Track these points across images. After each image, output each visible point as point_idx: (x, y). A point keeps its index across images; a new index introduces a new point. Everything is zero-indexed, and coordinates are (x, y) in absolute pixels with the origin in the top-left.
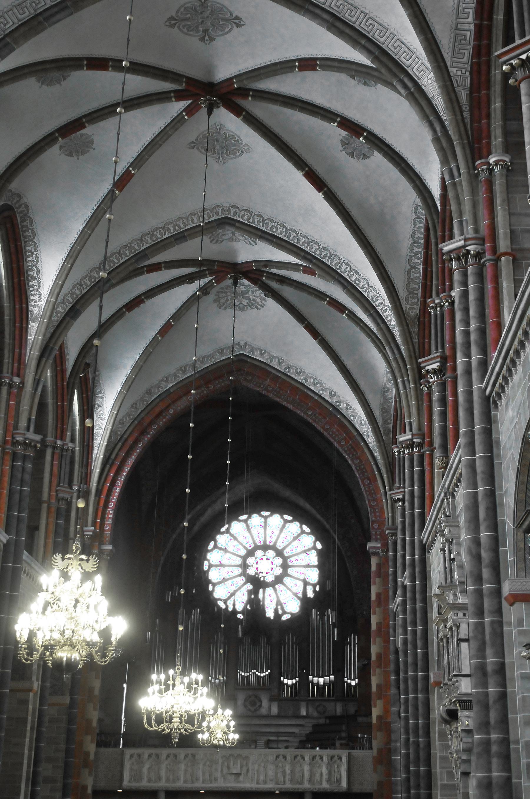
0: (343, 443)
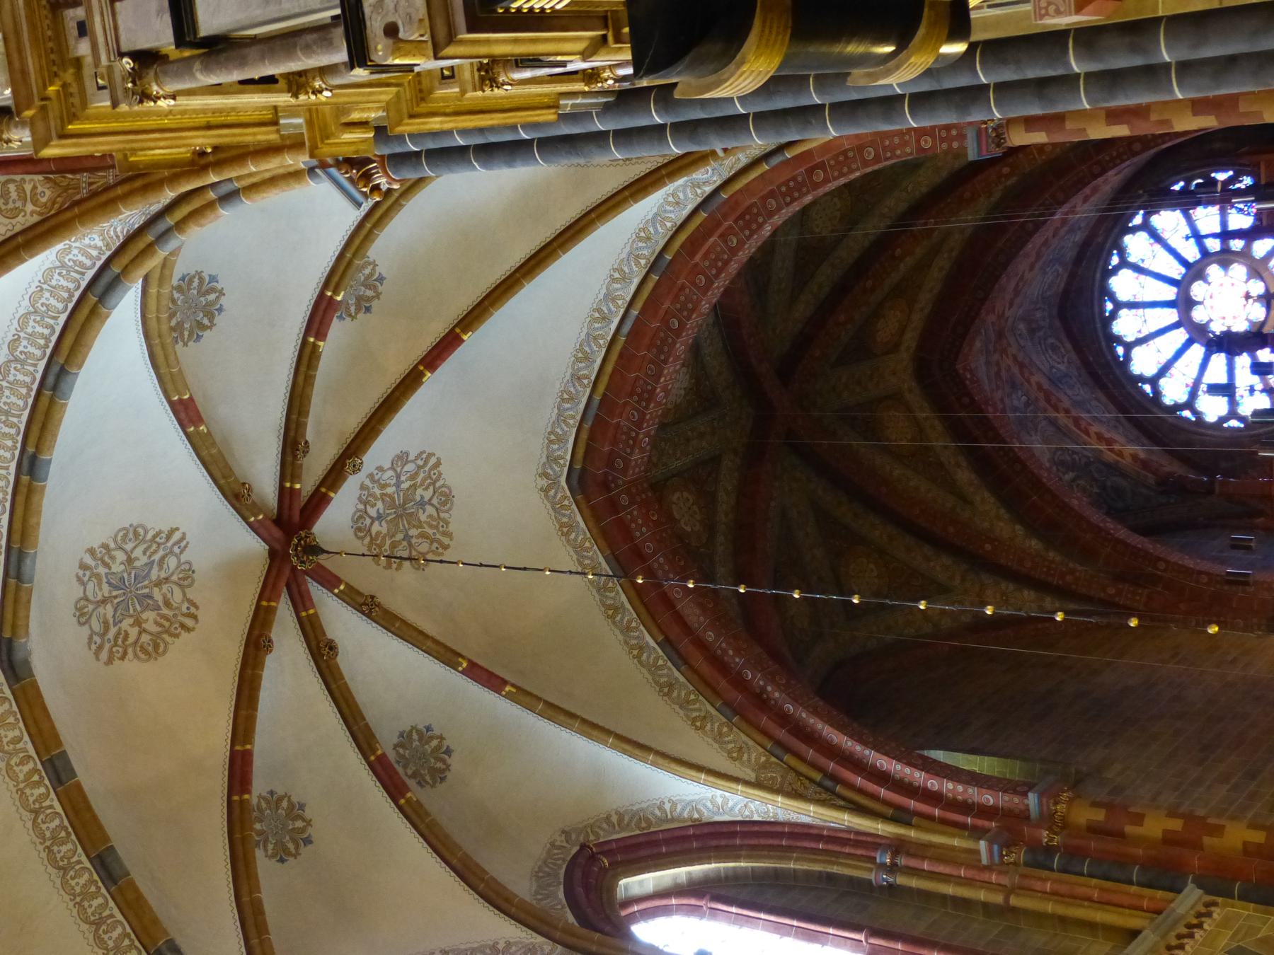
0: (734, 241)
